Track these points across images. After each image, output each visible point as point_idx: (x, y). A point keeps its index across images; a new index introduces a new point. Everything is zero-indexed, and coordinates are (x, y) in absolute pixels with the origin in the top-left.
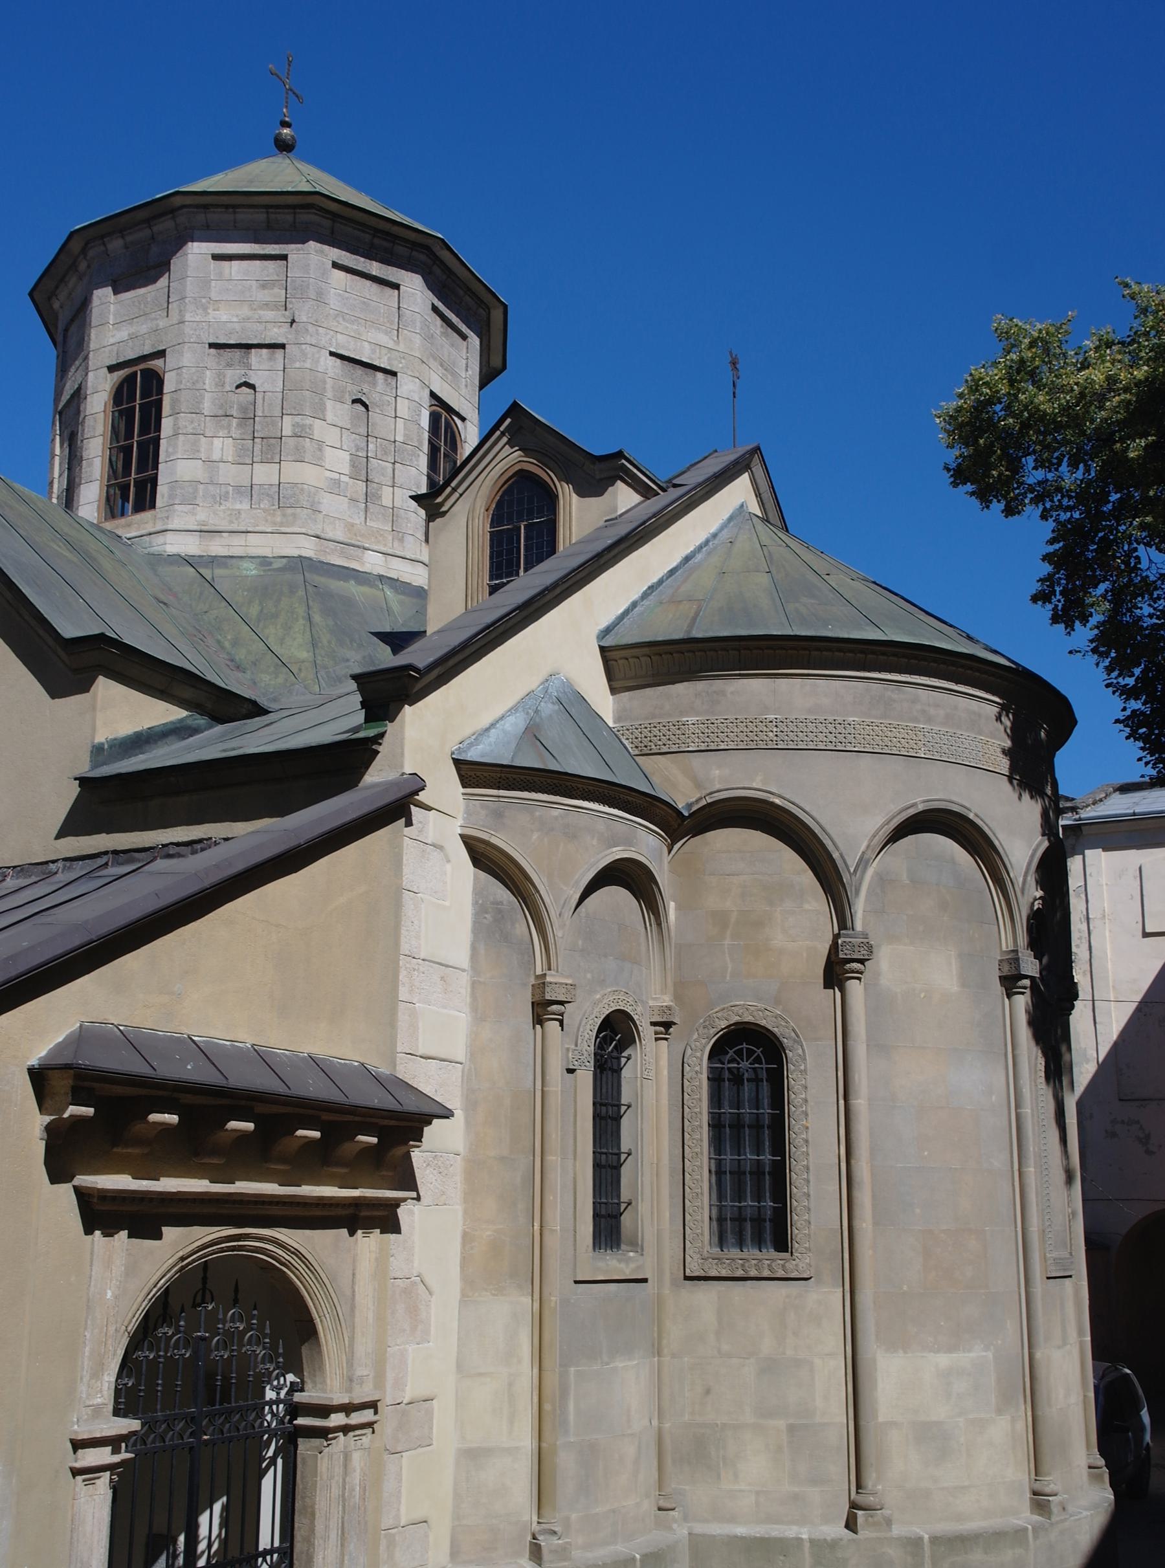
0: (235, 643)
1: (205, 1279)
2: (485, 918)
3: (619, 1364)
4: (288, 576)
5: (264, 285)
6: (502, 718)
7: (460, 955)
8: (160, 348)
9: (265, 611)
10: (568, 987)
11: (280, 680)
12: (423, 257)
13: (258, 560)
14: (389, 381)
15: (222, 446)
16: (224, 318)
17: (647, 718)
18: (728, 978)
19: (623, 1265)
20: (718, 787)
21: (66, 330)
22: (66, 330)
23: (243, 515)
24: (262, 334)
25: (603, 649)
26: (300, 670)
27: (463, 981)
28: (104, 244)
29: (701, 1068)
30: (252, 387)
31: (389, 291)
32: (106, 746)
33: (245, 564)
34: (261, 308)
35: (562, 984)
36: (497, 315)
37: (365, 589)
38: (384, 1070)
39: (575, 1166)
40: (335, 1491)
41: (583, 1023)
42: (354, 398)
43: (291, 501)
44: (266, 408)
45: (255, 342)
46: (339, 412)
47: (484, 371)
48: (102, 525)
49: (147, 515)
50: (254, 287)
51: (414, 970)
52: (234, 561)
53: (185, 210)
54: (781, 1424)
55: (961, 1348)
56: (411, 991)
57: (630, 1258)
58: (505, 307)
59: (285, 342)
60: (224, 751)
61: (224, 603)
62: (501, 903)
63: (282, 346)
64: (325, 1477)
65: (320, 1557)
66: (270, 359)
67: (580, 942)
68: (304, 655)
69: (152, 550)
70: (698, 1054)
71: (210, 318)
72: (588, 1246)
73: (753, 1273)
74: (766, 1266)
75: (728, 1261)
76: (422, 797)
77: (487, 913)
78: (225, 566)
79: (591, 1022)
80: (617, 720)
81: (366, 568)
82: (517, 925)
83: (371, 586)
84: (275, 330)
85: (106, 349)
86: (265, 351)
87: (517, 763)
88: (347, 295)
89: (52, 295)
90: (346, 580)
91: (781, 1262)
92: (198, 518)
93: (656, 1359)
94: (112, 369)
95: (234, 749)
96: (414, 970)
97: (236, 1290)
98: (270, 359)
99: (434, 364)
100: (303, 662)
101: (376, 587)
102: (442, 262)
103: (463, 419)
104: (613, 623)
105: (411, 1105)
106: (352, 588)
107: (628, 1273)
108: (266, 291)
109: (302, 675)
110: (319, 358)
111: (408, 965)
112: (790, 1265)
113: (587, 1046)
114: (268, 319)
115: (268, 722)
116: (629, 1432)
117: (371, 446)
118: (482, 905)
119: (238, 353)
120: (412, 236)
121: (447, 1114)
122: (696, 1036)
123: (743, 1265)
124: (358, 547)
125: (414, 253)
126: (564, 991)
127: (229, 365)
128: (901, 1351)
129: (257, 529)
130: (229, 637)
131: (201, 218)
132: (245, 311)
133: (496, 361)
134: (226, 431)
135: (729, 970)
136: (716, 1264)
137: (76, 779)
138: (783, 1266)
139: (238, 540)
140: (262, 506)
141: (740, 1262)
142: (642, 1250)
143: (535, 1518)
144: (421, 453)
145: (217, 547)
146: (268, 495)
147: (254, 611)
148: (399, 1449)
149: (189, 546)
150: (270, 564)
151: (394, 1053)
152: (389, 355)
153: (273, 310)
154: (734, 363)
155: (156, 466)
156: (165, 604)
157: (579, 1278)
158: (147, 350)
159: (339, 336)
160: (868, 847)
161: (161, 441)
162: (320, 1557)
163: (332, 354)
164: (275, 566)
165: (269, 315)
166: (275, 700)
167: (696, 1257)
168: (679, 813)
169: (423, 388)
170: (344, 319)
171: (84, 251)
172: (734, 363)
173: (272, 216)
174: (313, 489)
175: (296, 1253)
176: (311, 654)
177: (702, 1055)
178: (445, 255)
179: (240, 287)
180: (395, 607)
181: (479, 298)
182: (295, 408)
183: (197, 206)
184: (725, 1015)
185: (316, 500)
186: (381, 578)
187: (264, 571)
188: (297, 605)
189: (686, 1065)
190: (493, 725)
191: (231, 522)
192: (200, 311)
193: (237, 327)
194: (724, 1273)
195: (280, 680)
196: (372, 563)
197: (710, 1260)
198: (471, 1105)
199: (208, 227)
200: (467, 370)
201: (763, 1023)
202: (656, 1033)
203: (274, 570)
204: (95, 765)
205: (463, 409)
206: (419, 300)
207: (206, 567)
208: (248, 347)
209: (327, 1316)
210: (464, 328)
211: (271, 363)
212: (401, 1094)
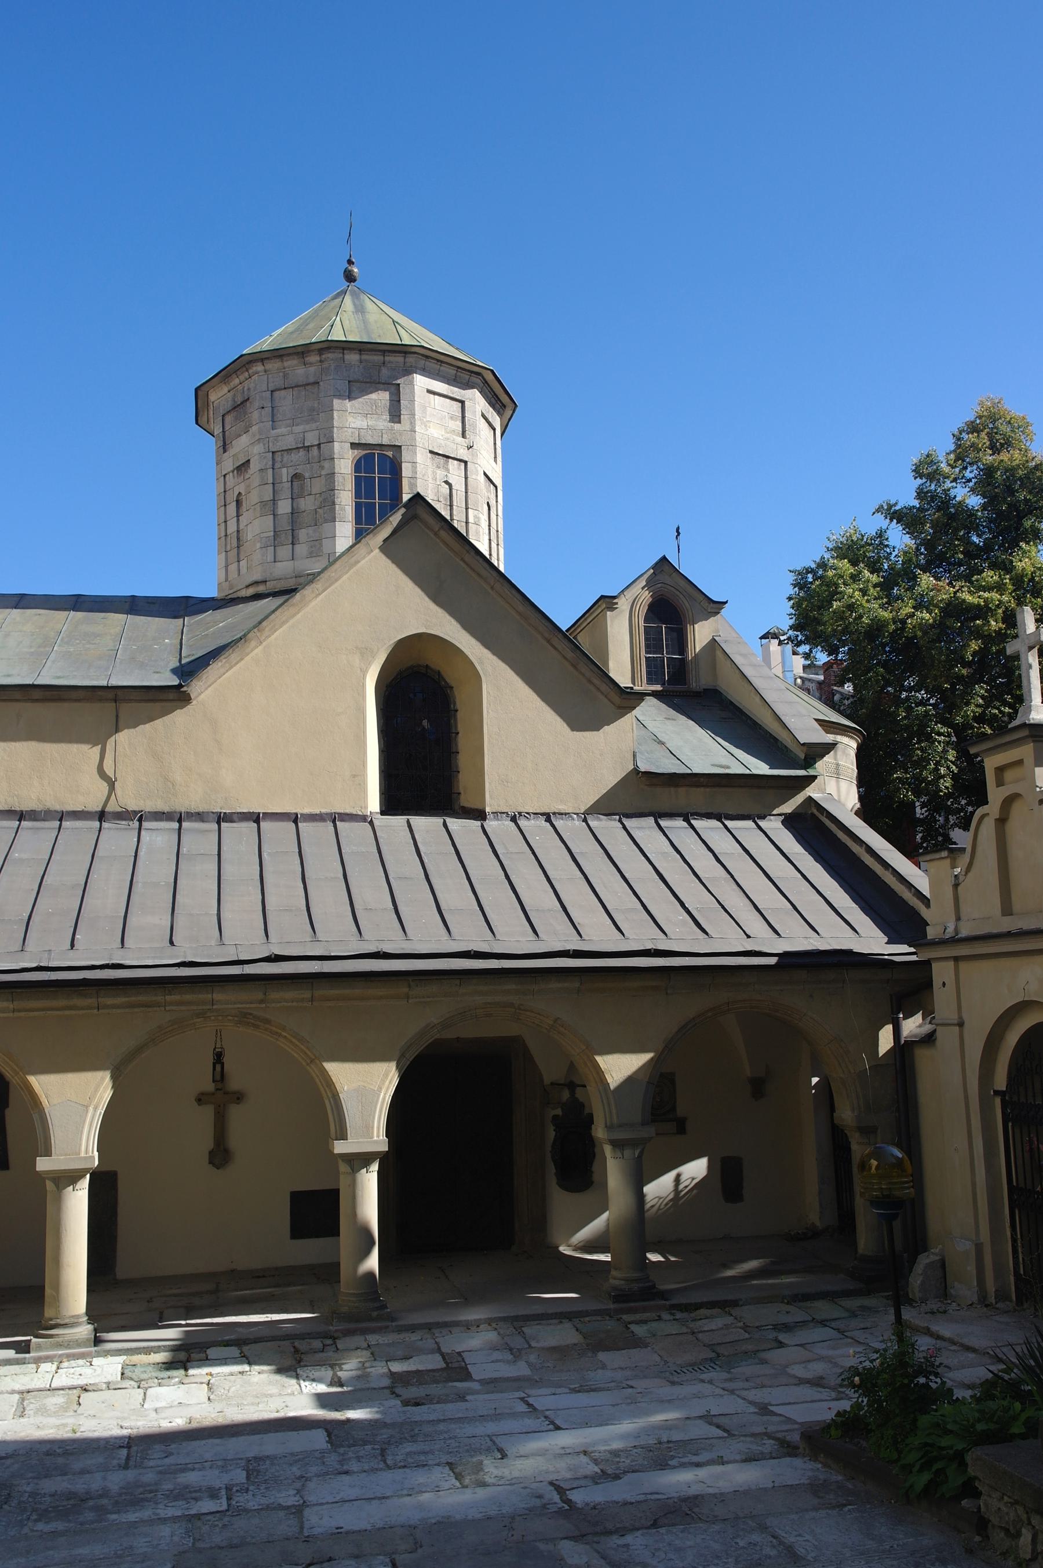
28: (343, 354)
45: (452, 456)
53: (416, 355)
59: (467, 459)
63: (466, 462)
66: (459, 469)
71: (427, 433)
85: (350, 430)
94: (354, 446)
119: (442, 460)
131: (422, 362)
163: (485, 474)
173: (459, 374)
183: (423, 355)
193: (442, 442)
199: (424, 370)
208: (448, 457)
210: (499, 459)
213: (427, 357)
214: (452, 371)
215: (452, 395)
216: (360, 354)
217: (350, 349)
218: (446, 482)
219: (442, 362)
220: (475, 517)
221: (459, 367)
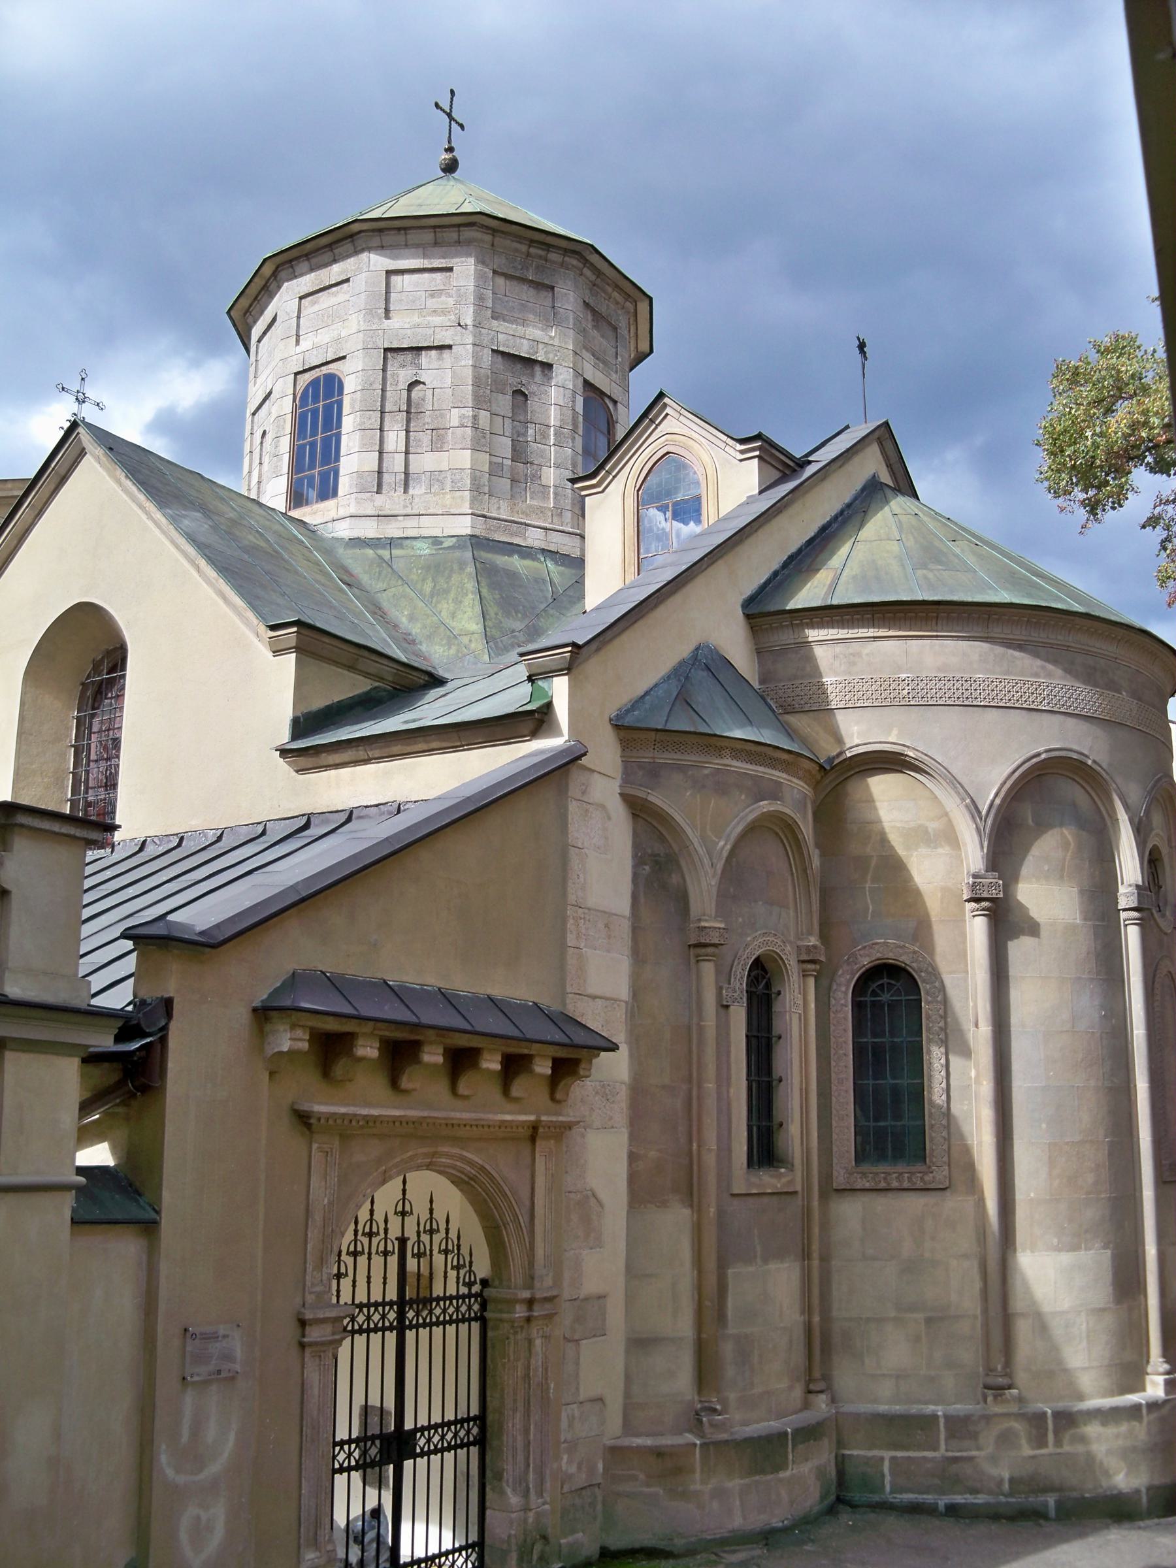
0: (411, 618)
1: (404, 1191)
2: (644, 869)
3: (772, 1266)
4: (457, 554)
5: (433, 294)
6: (656, 685)
7: (622, 904)
8: (341, 355)
9: (438, 588)
10: (721, 930)
11: (453, 651)
12: (575, 262)
13: (430, 540)
14: (546, 372)
15: (395, 439)
16: (397, 326)
17: (790, 680)
18: (869, 918)
19: (774, 1181)
20: (857, 741)
21: (259, 341)
22: (259, 341)
23: (416, 500)
24: (430, 337)
25: (748, 617)
26: (470, 641)
27: (625, 927)
28: (292, 267)
29: (847, 1001)
30: (424, 383)
31: (544, 294)
32: (302, 720)
33: (418, 544)
34: (430, 315)
35: (716, 928)
36: (643, 307)
37: (528, 562)
38: (556, 1007)
39: (728, 1092)
40: (520, 1372)
41: (735, 964)
42: (515, 389)
43: (459, 485)
44: (435, 403)
45: (425, 345)
46: (504, 403)
47: (632, 356)
48: (291, 514)
49: (330, 503)
50: (424, 297)
51: (581, 918)
52: (408, 542)
54: (920, 1316)
55: (1083, 1246)
56: (578, 938)
57: (781, 1173)
58: (651, 299)
59: (451, 343)
60: (406, 722)
61: (400, 582)
62: (658, 855)
63: (450, 347)
64: (512, 1358)
65: (510, 1425)
66: (439, 359)
67: (732, 890)
68: (475, 626)
69: (335, 535)
70: (843, 989)
71: (382, 327)
72: (742, 1164)
73: (895, 1184)
74: (906, 1178)
75: (871, 1175)
76: (584, 761)
77: (646, 864)
78: (401, 547)
79: (742, 962)
80: (762, 682)
81: (529, 542)
82: (673, 876)
83: (533, 560)
84: (444, 333)
86: (434, 353)
87: (670, 727)
88: (506, 298)
89: (247, 311)
90: (510, 554)
91: (918, 1175)
92: (376, 505)
93: (806, 1262)
94: (296, 374)
95: (414, 721)
96: (581, 918)
97: (431, 1202)
98: (439, 359)
99: (587, 355)
100: (473, 633)
101: (538, 560)
102: (592, 264)
103: (615, 402)
104: (756, 592)
105: (580, 1038)
106: (516, 563)
107: (779, 1186)
108: (434, 300)
109: (473, 645)
110: (482, 356)
111: (574, 915)
112: (927, 1178)
113: (740, 982)
114: (437, 324)
115: (444, 693)
116: (782, 1325)
117: (530, 432)
118: (641, 857)
119: (409, 356)
120: (563, 244)
121: (613, 1048)
122: (840, 972)
123: (885, 1179)
124: (521, 524)
125: (567, 259)
126: (717, 934)
127: (402, 366)
128: (1028, 1251)
129: (429, 512)
130: (406, 613)
132: (416, 319)
133: (644, 347)
134: (400, 425)
135: (870, 911)
136: (861, 1178)
137: (276, 750)
138: (921, 1178)
139: (413, 522)
140: (433, 491)
141: (883, 1175)
142: (793, 1165)
143: (696, 1398)
144: (576, 436)
145: (393, 530)
146: (438, 480)
147: (428, 587)
148: (576, 1337)
149: (369, 529)
150: (441, 543)
151: (564, 994)
152: (545, 349)
153: (440, 316)
154: (862, 346)
155: (337, 459)
156: (349, 585)
157: (736, 1191)
158: (330, 357)
159: (501, 336)
160: (996, 795)
161: (343, 437)
162: (510, 1425)
163: (493, 350)
164: (445, 545)
165: (437, 320)
166: (448, 670)
167: (842, 1172)
168: (821, 767)
169: (577, 377)
170: (504, 320)
171: (275, 274)
172: (862, 346)
174: (478, 474)
175: (482, 1168)
176: (481, 626)
177: (847, 989)
178: (594, 258)
179: (411, 298)
180: (557, 579)
181: (626, 293)
182: (461, 402)
183: (373, 231)
184: (867, 952)
185: (481, 483)
186: (543, 550)
187: (436, 550)
188: (466, 580)
189: (831, 999)
190: (647, 693)
191: (405, 507)
192: (376, 321)
194: (867, 1185)
195: (453, 651)
196: (534, 538)
197: (855, 1175)
198: (635, 1040)
200: (617, 358)
201: (903, 958)
202: (803, 971)
203: (444, 548)
204: (295, 737)
205: (614, 393)
206: (572, 299)
207: (383, 547)
208: (419, 349)
209: (511, 1224)
211: (441, 362)
212: (570, 1029)
213: (381, 230)
214: (428, 236)
215: (430, 266)
216: (308, 260)
217: (297, 258)
218: (417, 383)
219: (405, 229)
220: (462, 417)
221: (435, 227)
